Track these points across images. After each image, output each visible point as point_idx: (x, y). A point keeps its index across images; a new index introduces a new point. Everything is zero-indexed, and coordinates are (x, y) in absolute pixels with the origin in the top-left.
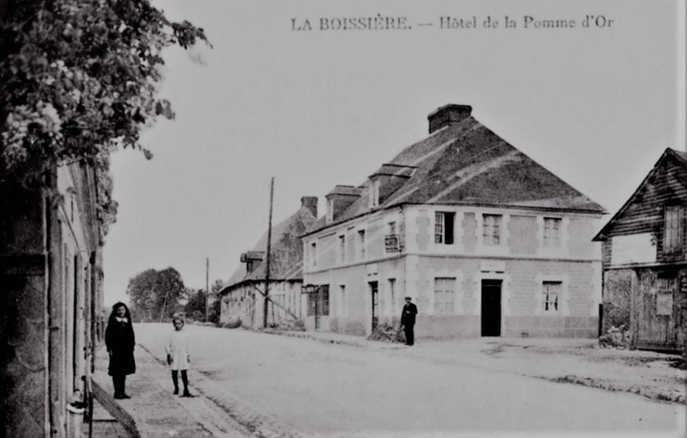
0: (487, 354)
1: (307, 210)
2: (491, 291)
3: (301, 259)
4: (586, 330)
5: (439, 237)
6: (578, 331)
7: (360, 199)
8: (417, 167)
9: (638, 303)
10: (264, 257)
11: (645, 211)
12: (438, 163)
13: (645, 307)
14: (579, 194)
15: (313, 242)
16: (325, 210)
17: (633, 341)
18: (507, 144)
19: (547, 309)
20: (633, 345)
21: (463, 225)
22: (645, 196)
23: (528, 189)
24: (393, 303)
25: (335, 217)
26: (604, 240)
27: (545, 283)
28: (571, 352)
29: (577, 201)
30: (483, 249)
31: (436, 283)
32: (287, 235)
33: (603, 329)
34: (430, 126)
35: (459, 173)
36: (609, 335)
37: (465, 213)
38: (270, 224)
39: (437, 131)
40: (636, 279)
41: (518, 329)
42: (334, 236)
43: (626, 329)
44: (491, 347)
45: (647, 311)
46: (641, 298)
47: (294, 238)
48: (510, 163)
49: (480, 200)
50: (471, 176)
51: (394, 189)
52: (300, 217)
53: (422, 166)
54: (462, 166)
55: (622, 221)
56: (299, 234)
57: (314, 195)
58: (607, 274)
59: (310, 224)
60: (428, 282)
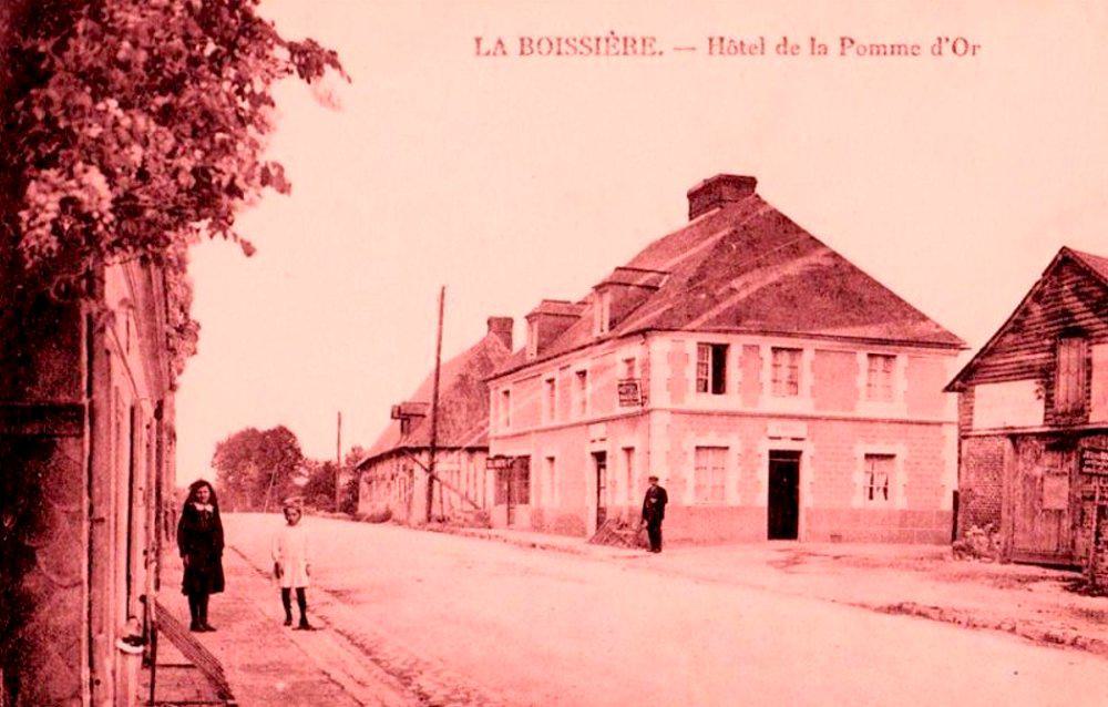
0: (776, 567)
1: (497, 338)
2: (784, 469)
3: (486, 414)
4: (932, 532)
5: (702, 383)
6: (919, 533)
7: (579, 322)
8: (670, 273)
9: (1015, 490)
10: (429, 411)
11: (1027, 346)
12: (702, 267)
13: (1024, 495)
14: (924, 318)
15: (505, 389)
16: (522, 337)
17: (1005, 550)
18: (812, 238)
19: (871, 497)
20: (1005, 555)
21: (742, 364)
22: (1026, 322)
23: (844, 308)
24: (630, 487)
25: (540, 349)
26: (961, 390)
27: (869, 456)
28: (908, 567)
29: (919, 330)
30: (771, 402)
31: (697, 455)
32: (464, 378)
33: (959, 531)
34: (691, 208)
35: (736, 283)
36: (968, 540)
37: (745, 346)
38: (439, 359)
39: (702, 217)
40: (1012, 453)
41: (825, 528)
42: (538, 380)
43: (994, 530)
44: (783, 556)
45: (1028, 503)
46: (1019, 482)
47: (475, 382)
48: (815, 268)
49: (768, 326)
50: (754, 288)
51: (634, 306)
52: (485, 349)
53: (678, 271)
54: (741, 272)
55: (989, 361)
56: (486, 372)
57: (508, 315)
58: (965, 443)
59: (501, 360)
60: (685, 454)
